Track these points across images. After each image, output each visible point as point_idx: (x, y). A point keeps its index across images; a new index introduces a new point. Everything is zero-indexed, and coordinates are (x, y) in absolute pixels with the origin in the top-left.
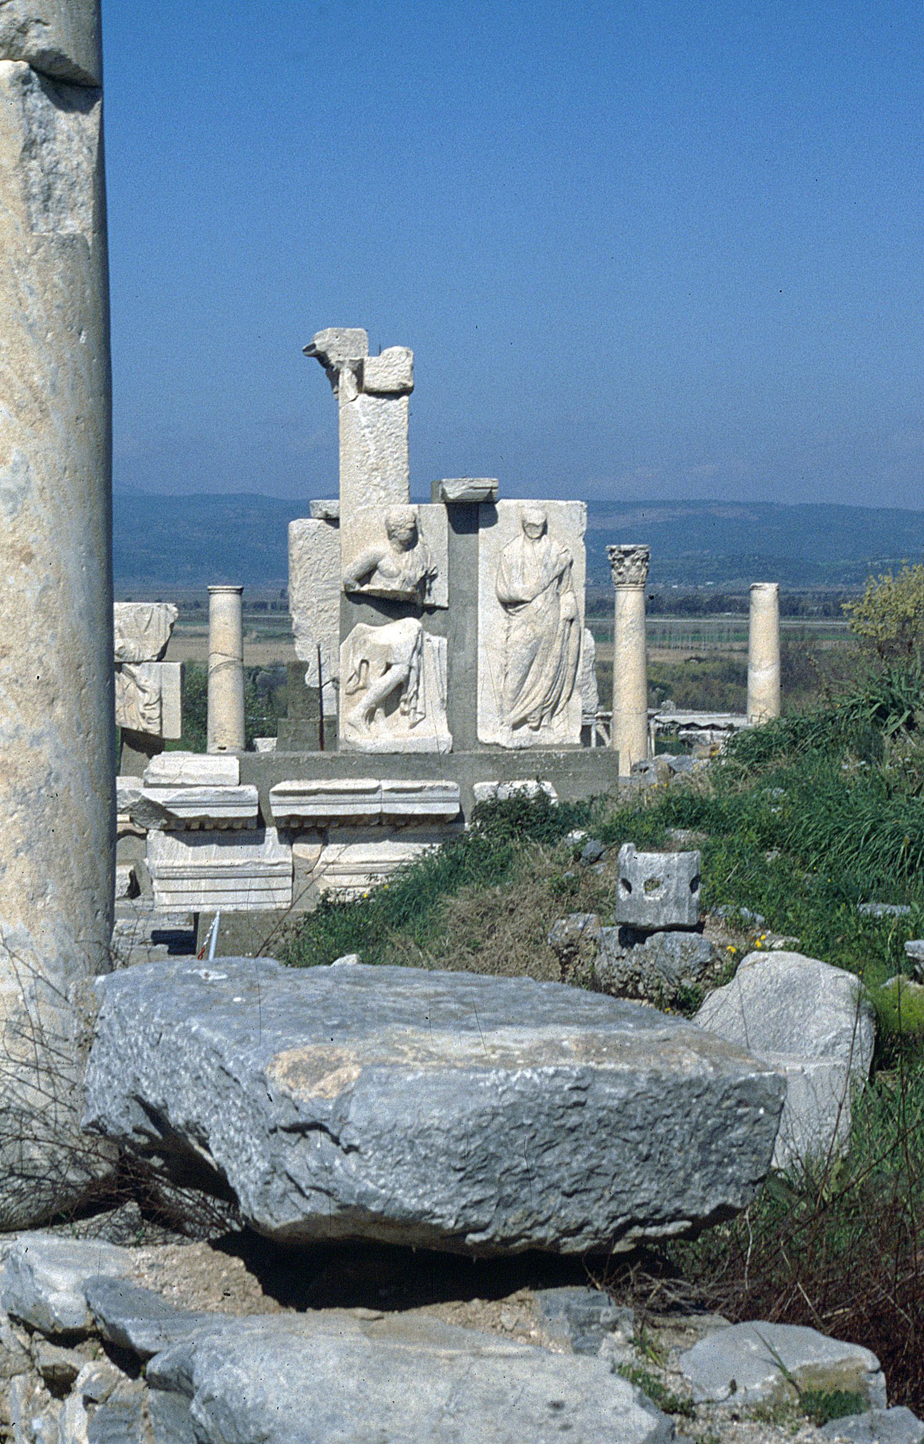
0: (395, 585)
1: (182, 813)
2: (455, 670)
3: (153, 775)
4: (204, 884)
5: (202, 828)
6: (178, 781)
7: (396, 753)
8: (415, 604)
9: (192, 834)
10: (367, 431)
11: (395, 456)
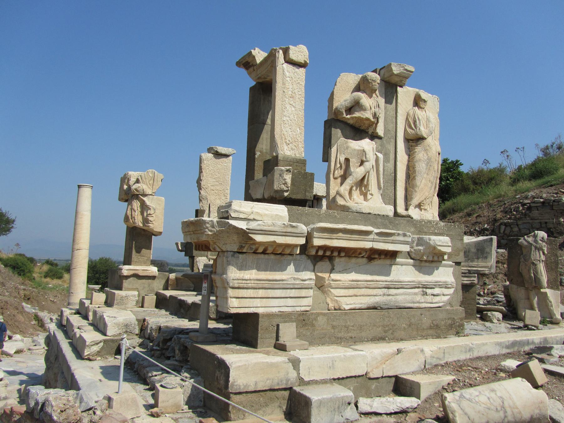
0: (368, 115)
1: (259, 238)
2: (386, 173)
3: (236, 211)
4: (261, 293)
5: (264, 252)
6: (251, 217)
7: (369, 214)
8: (367, 133)
9: (255, 256)
10: (288, 79)
11: (300, 93)
